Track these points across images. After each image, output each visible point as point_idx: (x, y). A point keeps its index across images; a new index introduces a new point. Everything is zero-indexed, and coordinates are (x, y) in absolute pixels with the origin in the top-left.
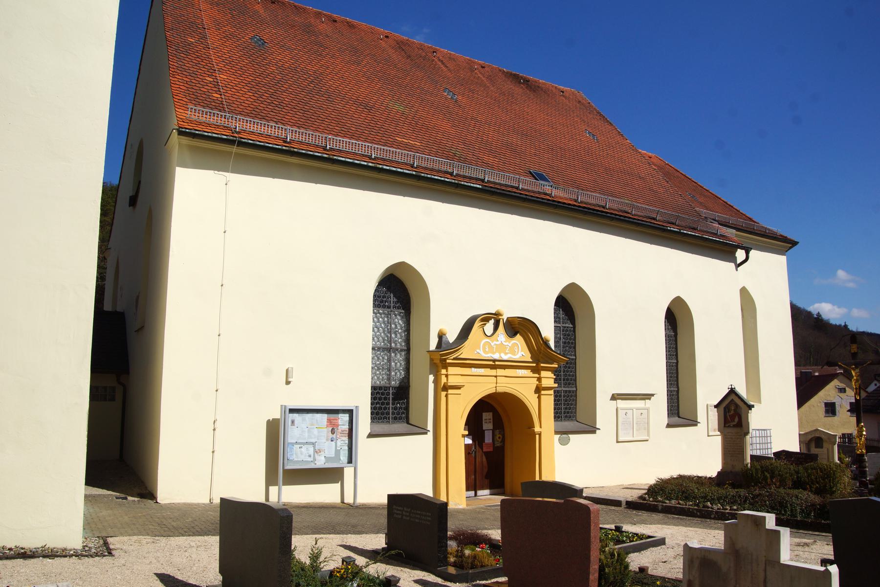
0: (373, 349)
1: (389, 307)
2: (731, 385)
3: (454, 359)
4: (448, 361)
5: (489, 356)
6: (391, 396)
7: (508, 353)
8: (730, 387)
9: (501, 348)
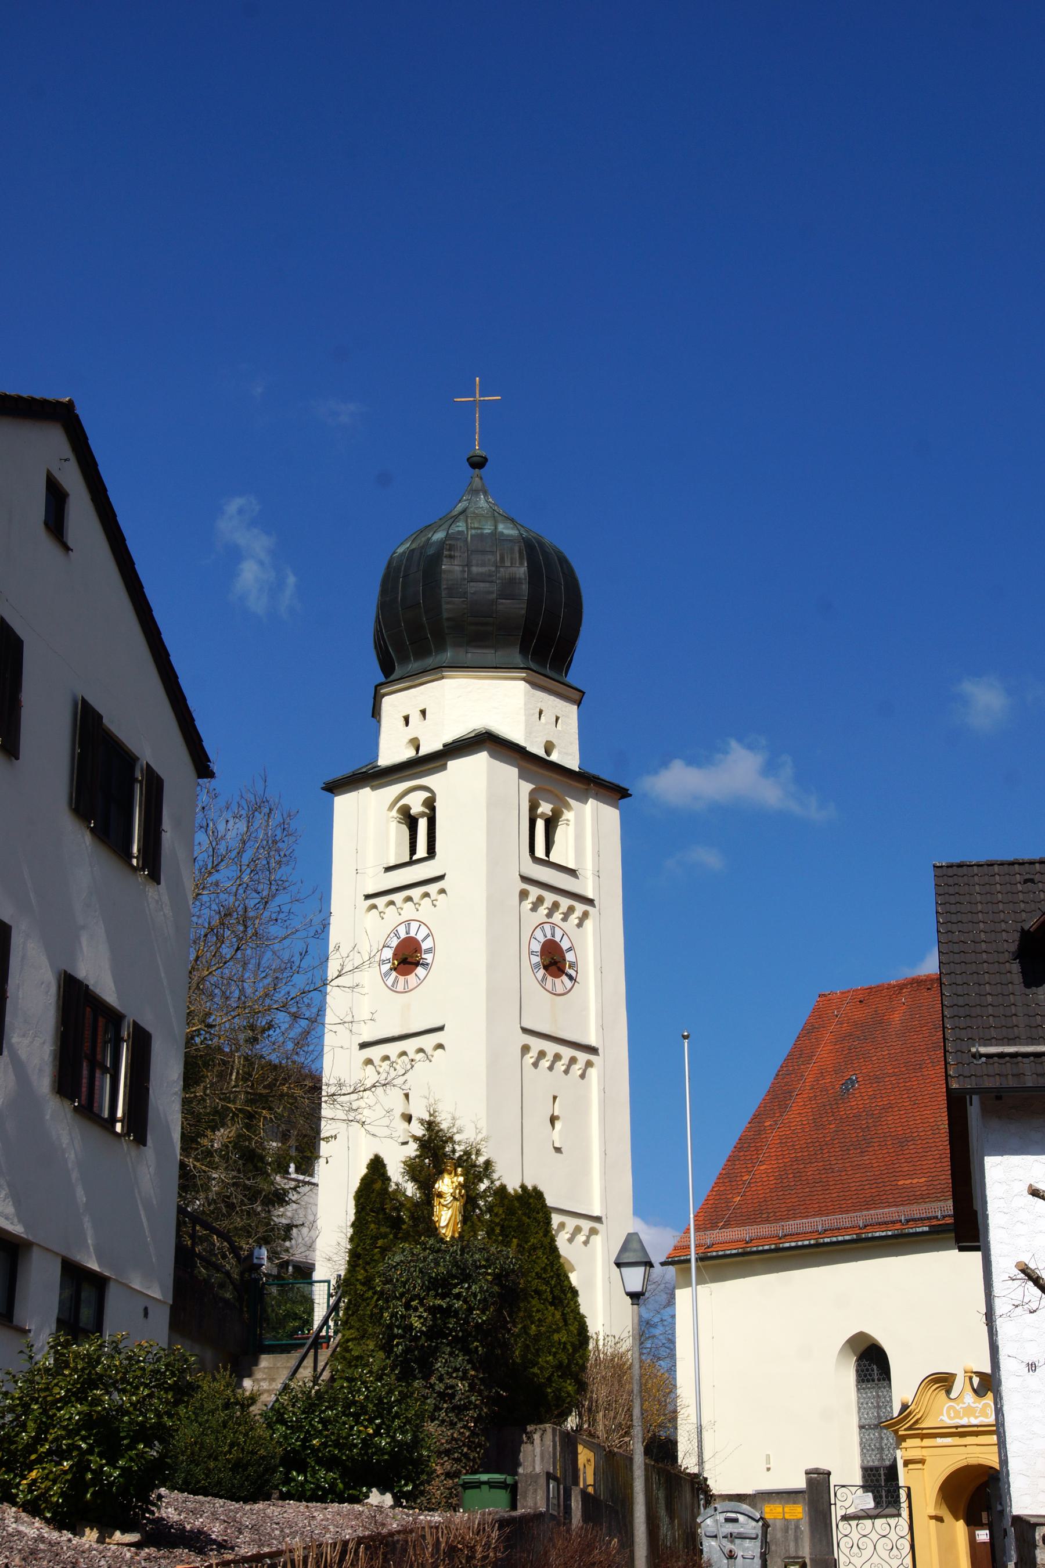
0: (861, 1427)
1: (873, 1380)
3: (906, 1430)
4: (900, 1433)
5: (949, 1422)
6: (883, 1477)
7: (978, 1417)
9: (969, 1411)
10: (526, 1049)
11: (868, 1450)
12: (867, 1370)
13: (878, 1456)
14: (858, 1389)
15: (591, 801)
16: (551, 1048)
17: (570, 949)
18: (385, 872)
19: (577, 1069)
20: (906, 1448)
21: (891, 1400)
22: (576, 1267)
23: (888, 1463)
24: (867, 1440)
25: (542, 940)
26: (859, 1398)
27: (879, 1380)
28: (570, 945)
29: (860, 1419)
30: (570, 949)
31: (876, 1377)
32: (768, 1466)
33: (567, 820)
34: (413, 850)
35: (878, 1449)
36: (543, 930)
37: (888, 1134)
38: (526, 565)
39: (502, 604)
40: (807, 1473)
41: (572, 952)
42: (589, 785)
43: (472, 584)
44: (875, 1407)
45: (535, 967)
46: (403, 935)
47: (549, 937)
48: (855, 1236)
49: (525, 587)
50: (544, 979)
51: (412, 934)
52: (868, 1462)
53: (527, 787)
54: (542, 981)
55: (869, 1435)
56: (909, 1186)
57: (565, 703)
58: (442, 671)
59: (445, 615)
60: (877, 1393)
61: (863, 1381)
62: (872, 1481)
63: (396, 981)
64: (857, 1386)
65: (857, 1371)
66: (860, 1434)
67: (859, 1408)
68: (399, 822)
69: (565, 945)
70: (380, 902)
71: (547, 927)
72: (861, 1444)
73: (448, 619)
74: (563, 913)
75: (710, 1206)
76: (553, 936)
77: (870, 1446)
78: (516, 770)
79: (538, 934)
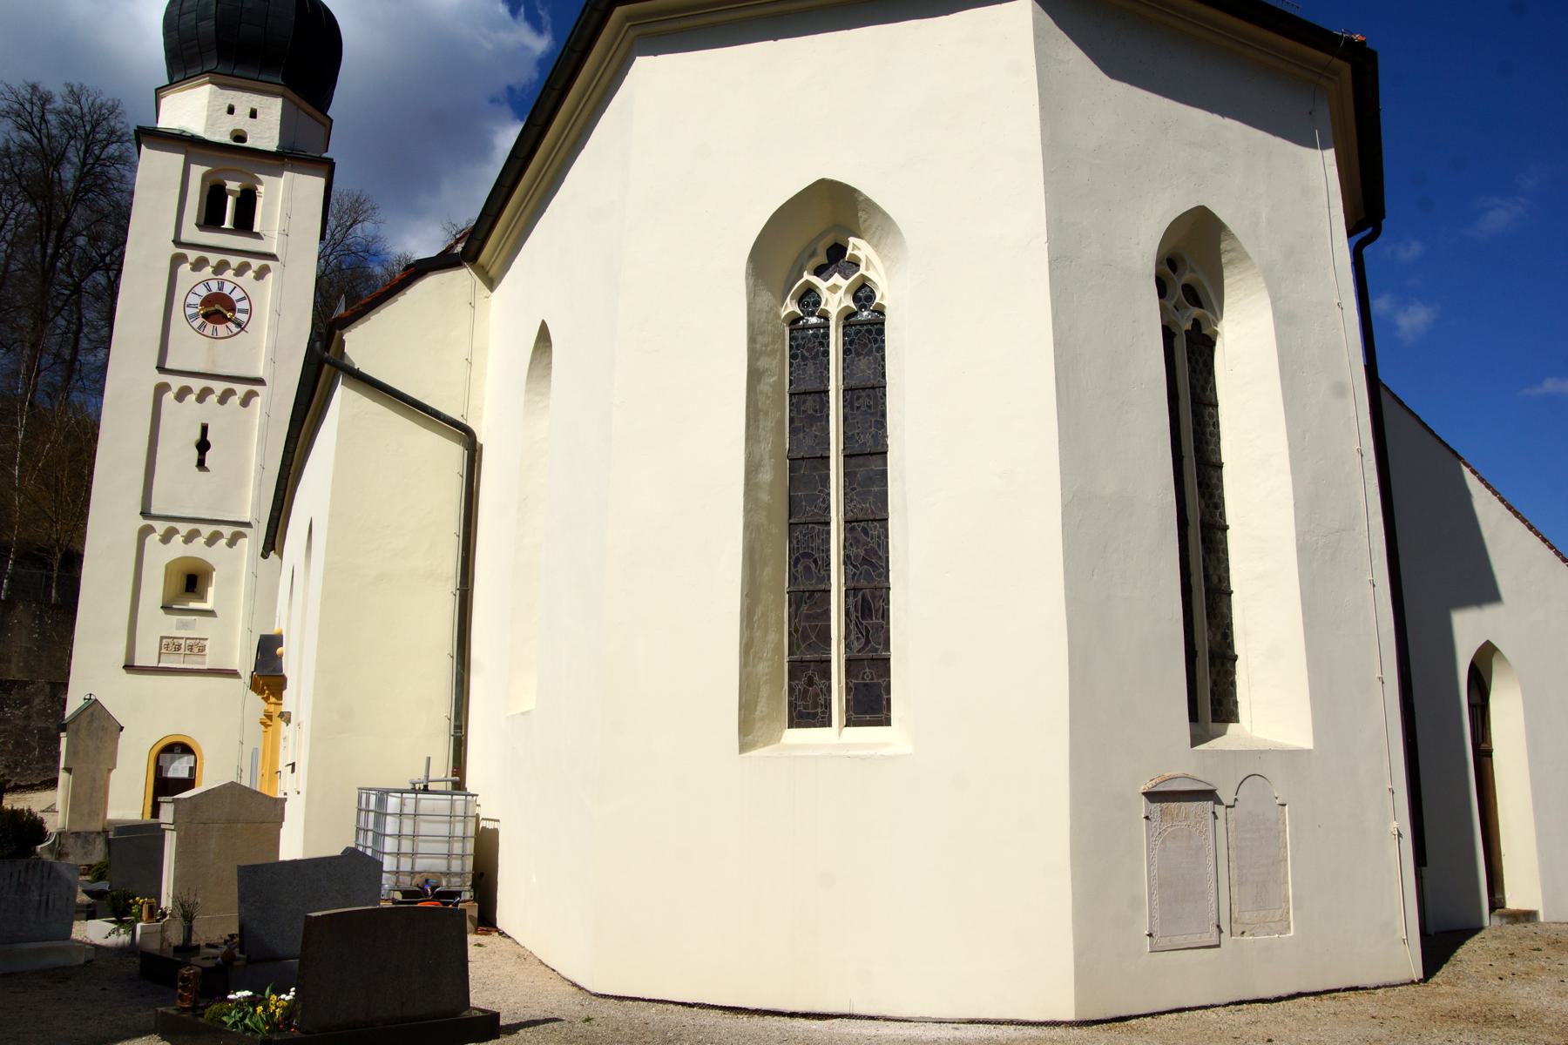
2: (91, 695)
8: (88, 697)
15: (285, 173)
16: (197, 384)
19: (235, 401)
22: (215, 567)
41: (247, 301)
42: (283, 160)
69: (235, 296)
76: (221, 288)
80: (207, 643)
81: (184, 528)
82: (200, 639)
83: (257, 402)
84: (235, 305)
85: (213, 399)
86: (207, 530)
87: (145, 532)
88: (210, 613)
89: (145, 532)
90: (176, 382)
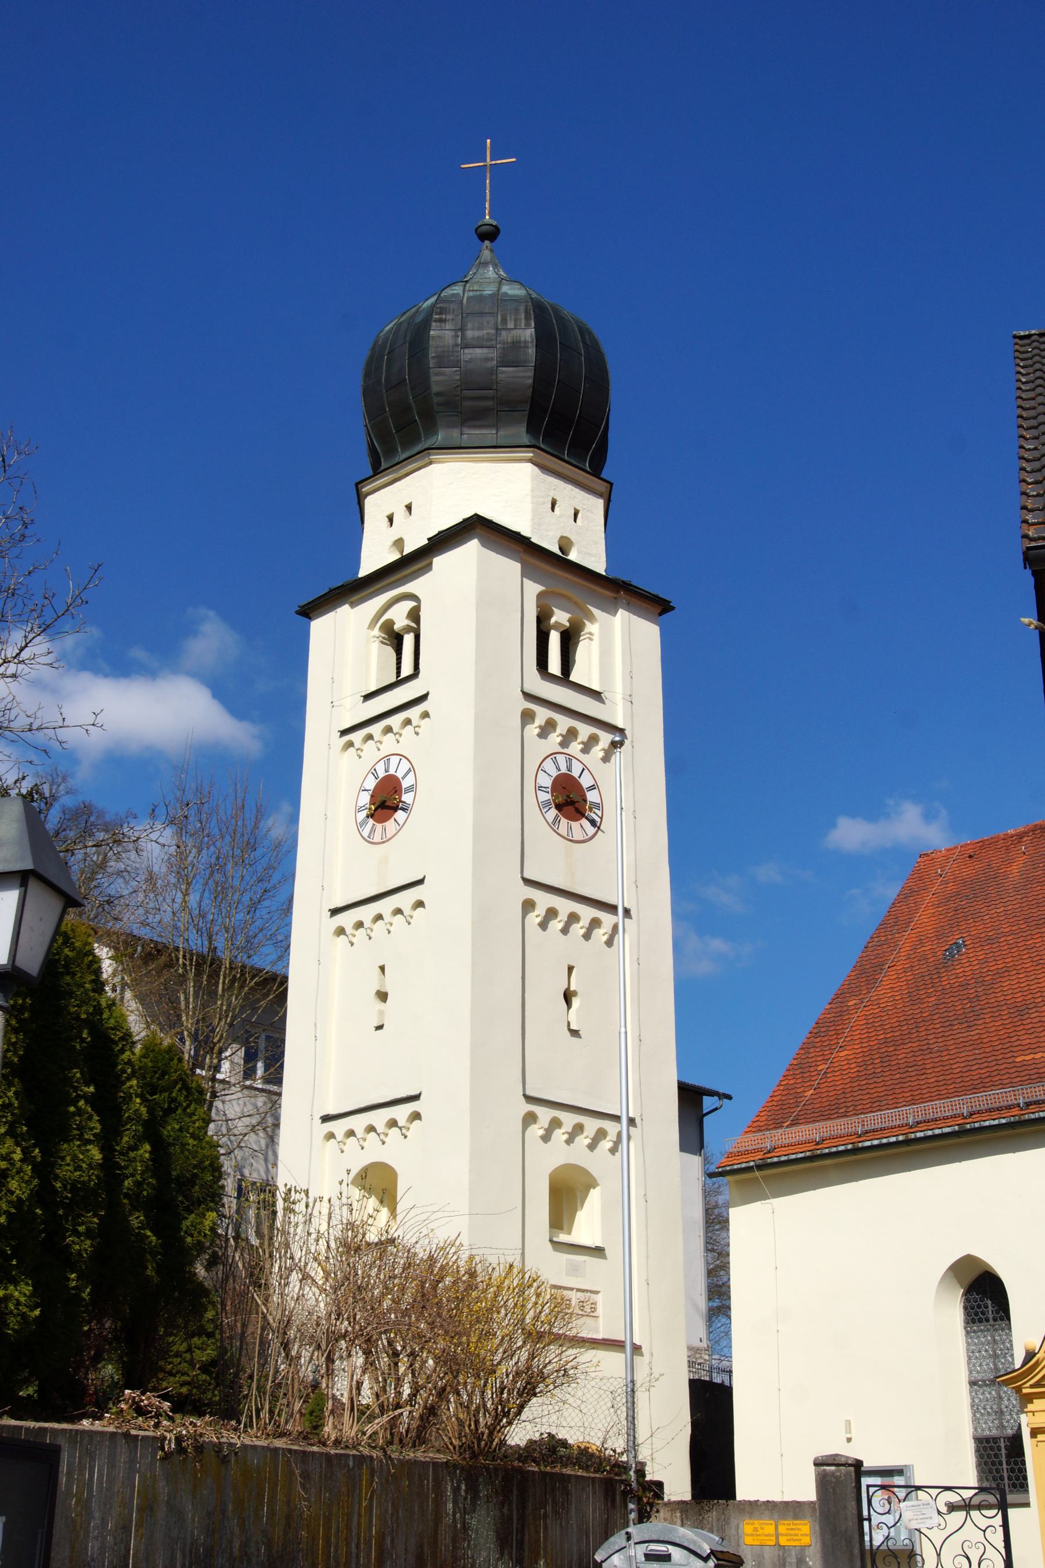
0: (973, 1383)
1: (987, 1320)
3: (1032, 1386)
4: (1025, 1391)
6: (1003, 1451)
10: (528, 906)
11: (982, 1415)
12: (979, 1306)
13: (996, 1422)
14: (967, 1333)
15: (620, 611)
16: (565, 907)
17: (592, 788)
18: (364, 701)
19: (600, 935)
20: (1033, 1412)
21: (1012, 1345)
22: (599, 1181)
23: (1010, 1432)
24: (980, 1401)
25: (554, 773)
26: (968, 1344)
27: (995, 1320)
28: (592, 783)
29: (971, 1372)
30: (592, 788)
31: (991, 1316)
32: (849, 1436)
33: (590, 634)
34: (398, 673)
35: (996, 1412)
36: (555, 761)
37: (1003, 1003)
38: (533, 325)
39: (503, 372)
40: (817, 1464)
41: (596, 791)
42: (618, 592)
43: (466, 351)
44: (990, 1356)
45: (543, 806)
46: (381, 774)
47: (564, 770)
48: (956, 1128)
49: (532, 351)
50: (556, 820)
51: (392, 772)
52: (983, 1430)
53: (533, 589)
54: (554, 823)
55: (983, 1394)
56: (1030, 1062)
57: (587, 495)
58: (430, 454)
59: (435, 389)
60: (993, 1337)
61: (973, 1321)
62: (989, 1456)
63: (373, 830)
64: (965, 1328)
65: (965, 1308)
66: (971, 1392)
67: (969, 1358)
68: (382, 642)
69: (586, 782)
70: (357, 737)
71: (561, 760)
72: (972, 1406)
73: (438, 394)
74: (582, 743)
75: (774, 1103)
76: (569, 769)
77: (985, 1409)
78: (519, 565)
79: (549, 765)
80: (599, 1299)
81: (569, 1120)
82: (592, 1292)
83: (626, 941)
84: (585, 795)
85: (578, 930)
86: (591, 1125)
87: (530, 1119)
88: (598, 1251)
89: (530, 1119)
90: (544, 901)
